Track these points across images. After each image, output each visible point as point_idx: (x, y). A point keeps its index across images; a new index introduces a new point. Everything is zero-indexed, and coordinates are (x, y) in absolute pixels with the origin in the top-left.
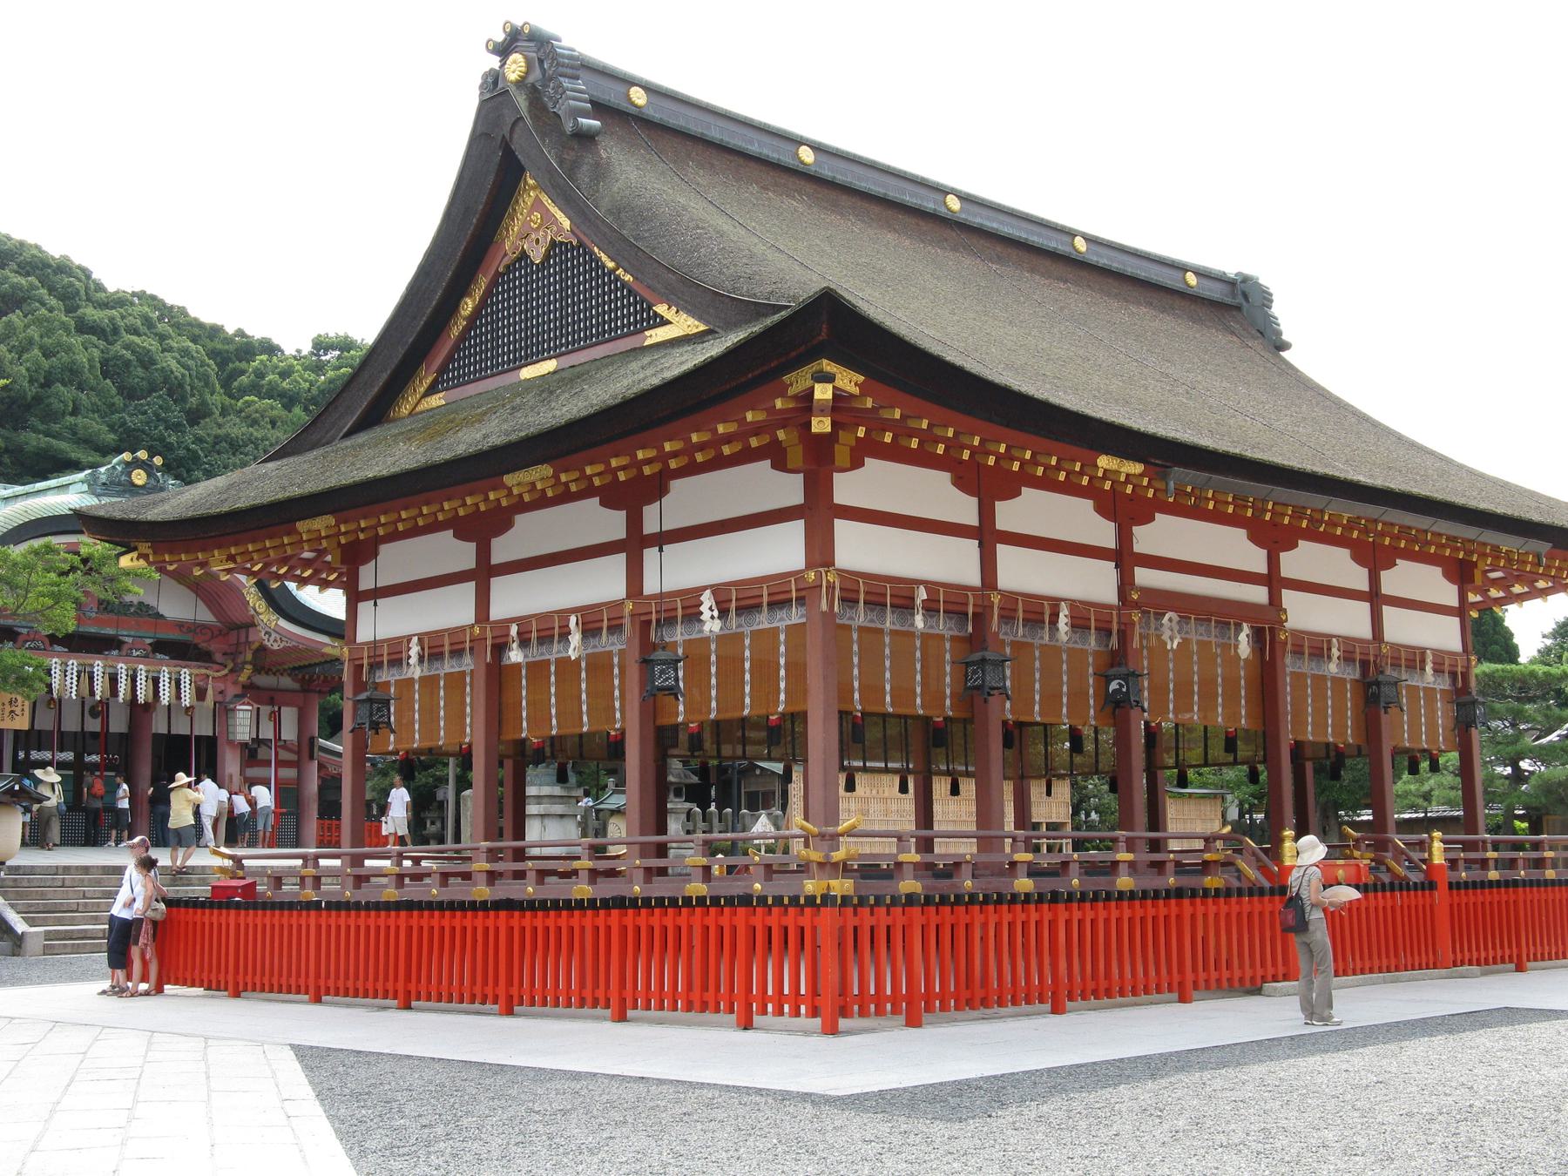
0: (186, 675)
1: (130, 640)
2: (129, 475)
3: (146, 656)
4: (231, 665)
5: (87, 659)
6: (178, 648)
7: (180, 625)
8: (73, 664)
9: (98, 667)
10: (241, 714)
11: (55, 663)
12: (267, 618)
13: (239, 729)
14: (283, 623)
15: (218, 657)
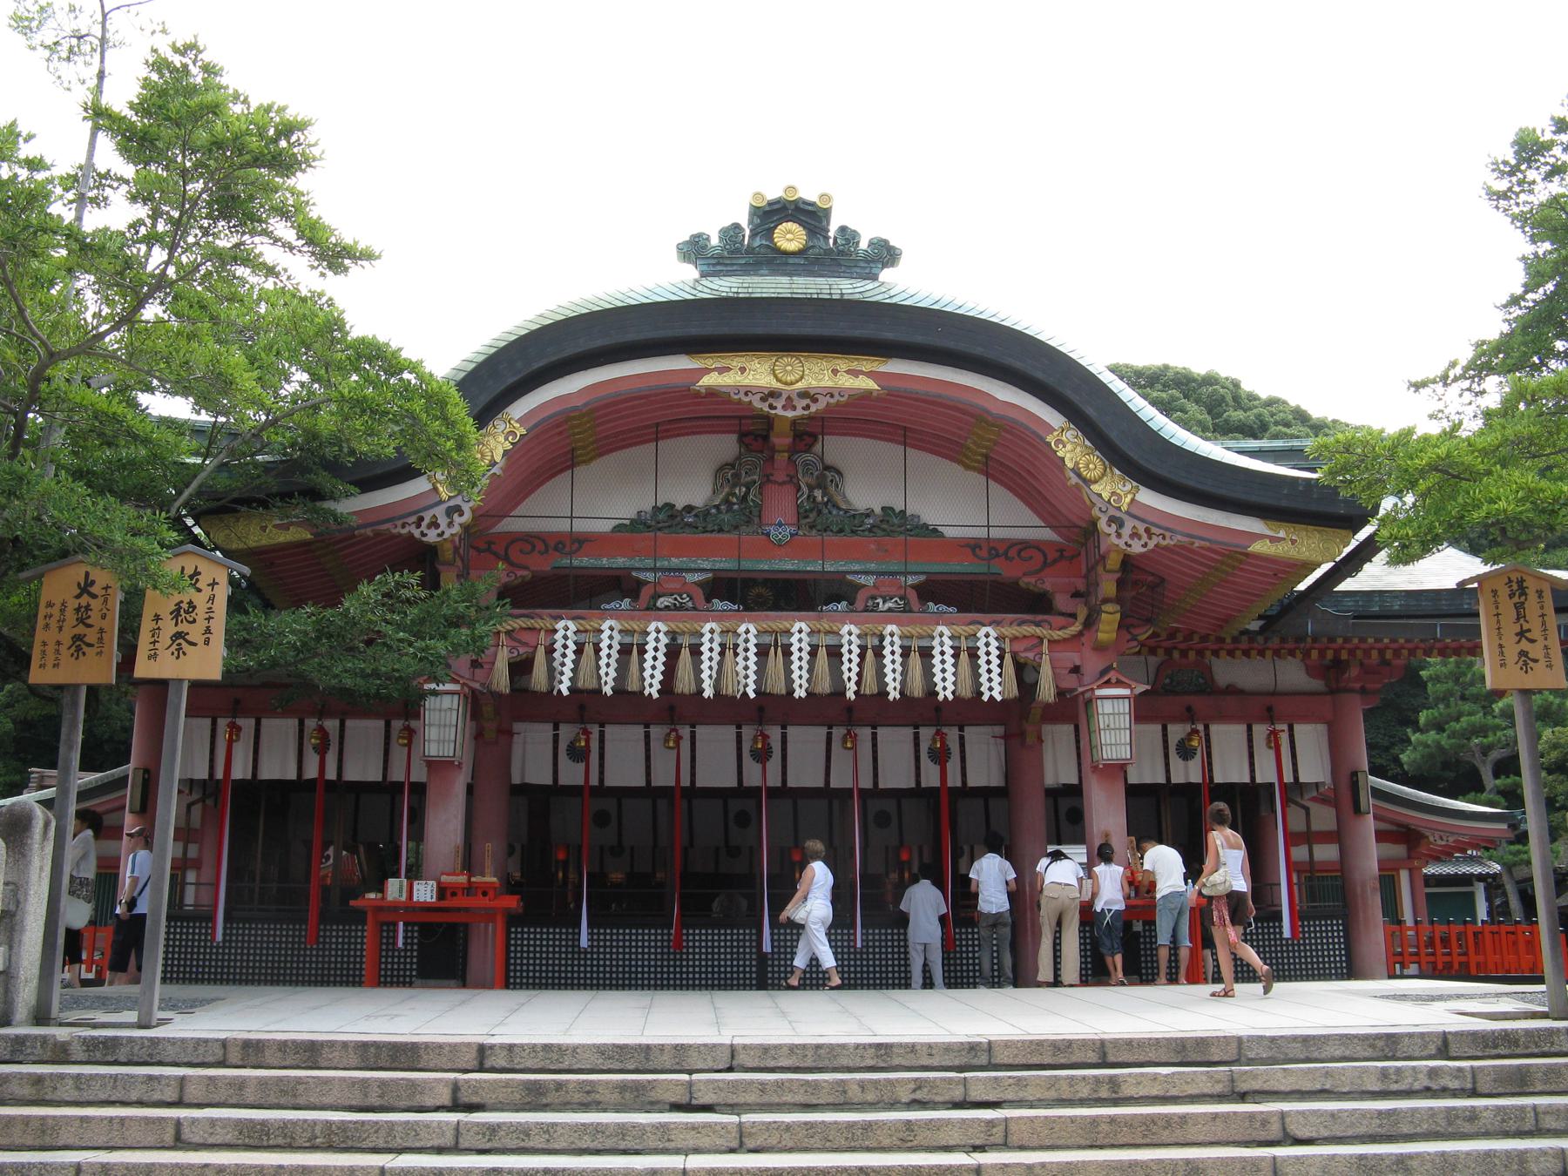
0: (988, 638)
1: (870, 581)
2: (770, 233)
3: (907, 609)
4: (1082, 613)
5: (776, 620)
6: (975, 587)
7: (973, 546)
8: (749, 631)
9: (800, 632)
10: (1105, 708)
11: (710, 633)
12: (1111, 489)
13: (1106, 737)
14: (1148, 497)
15: (1062, 602)
